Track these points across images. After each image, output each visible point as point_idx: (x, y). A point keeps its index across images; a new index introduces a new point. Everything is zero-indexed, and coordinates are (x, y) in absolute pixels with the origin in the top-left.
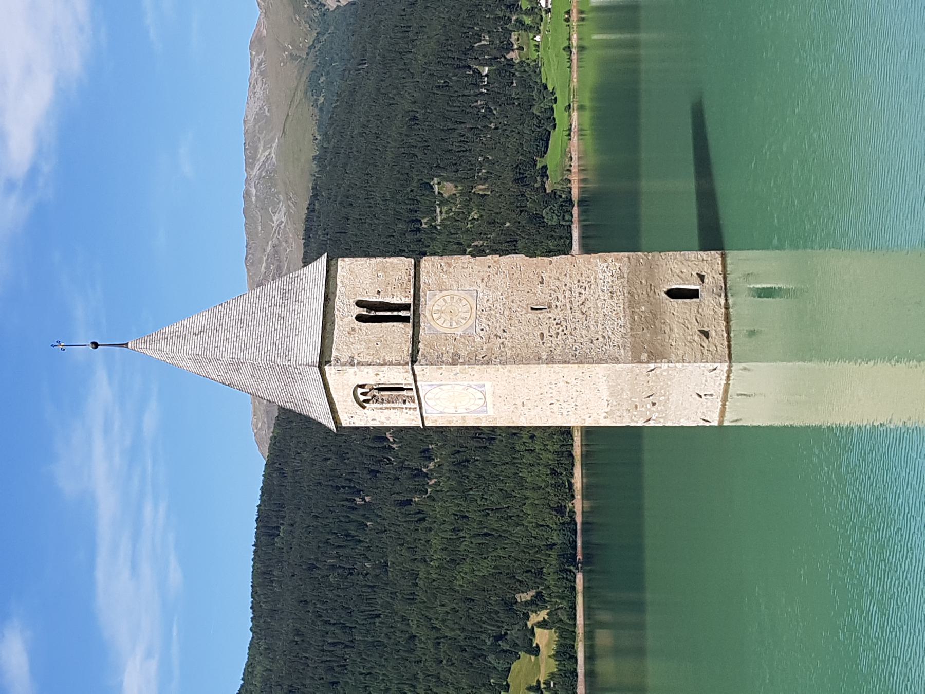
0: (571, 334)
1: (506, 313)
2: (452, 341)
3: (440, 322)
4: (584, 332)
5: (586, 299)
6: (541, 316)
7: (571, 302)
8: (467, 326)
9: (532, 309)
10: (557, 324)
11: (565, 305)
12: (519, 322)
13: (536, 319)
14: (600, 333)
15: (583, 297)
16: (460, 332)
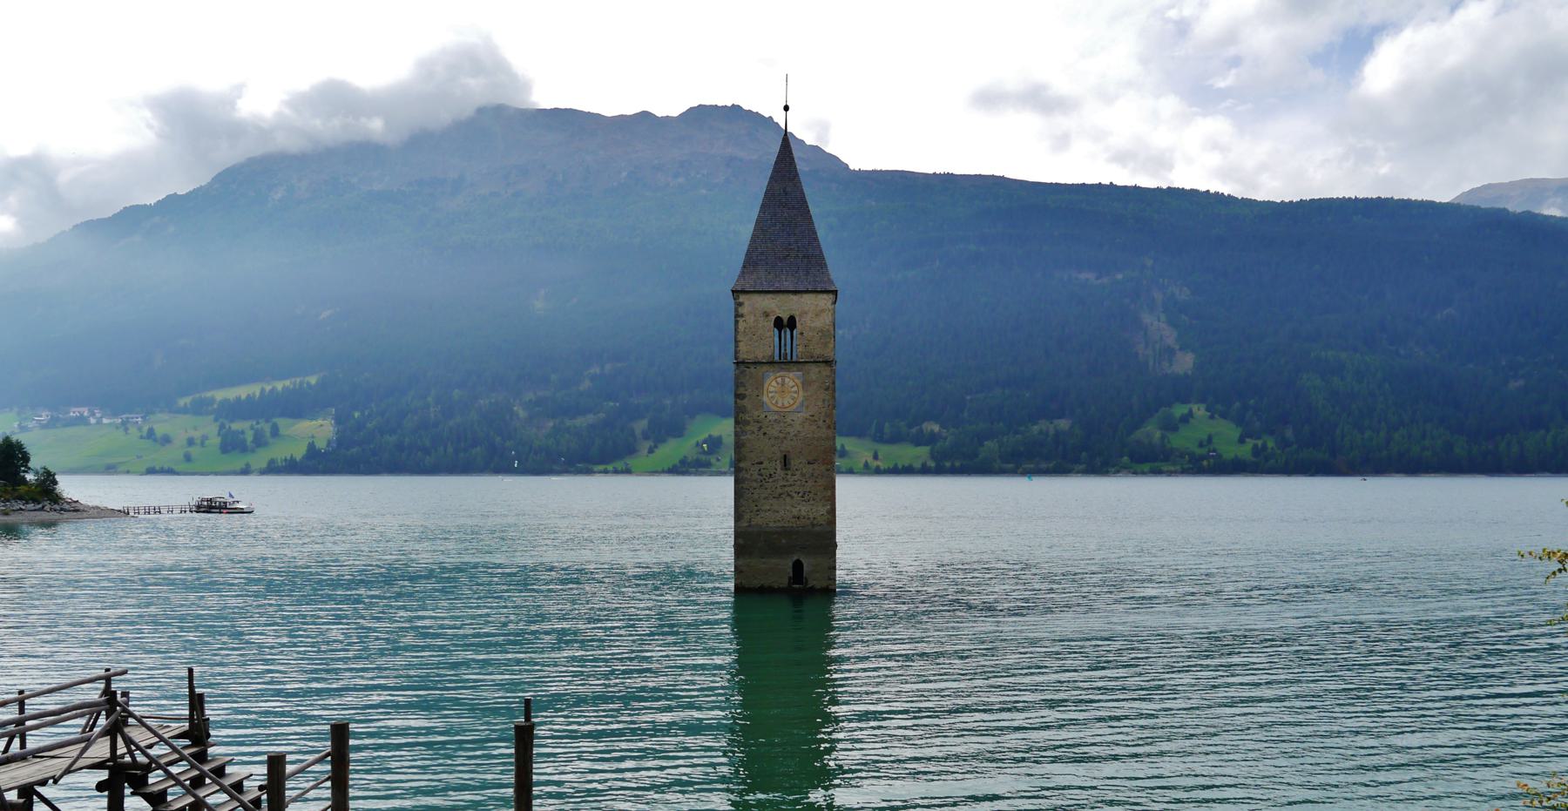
0: (761, 486)
1: (781, 435)
2: (756, 392)
3: (774, 383)
4: (763, 496)
5: (792, 497)
6: (778, 461)
7: (791, 485)
8: (770, 405)
9: (785, 456)
10: (771, 475)
11: (787, 481)
12: (773, 446)
13: (775, 458)
14: (763, 508)
15: (795, 495)
16: (765, 399)
